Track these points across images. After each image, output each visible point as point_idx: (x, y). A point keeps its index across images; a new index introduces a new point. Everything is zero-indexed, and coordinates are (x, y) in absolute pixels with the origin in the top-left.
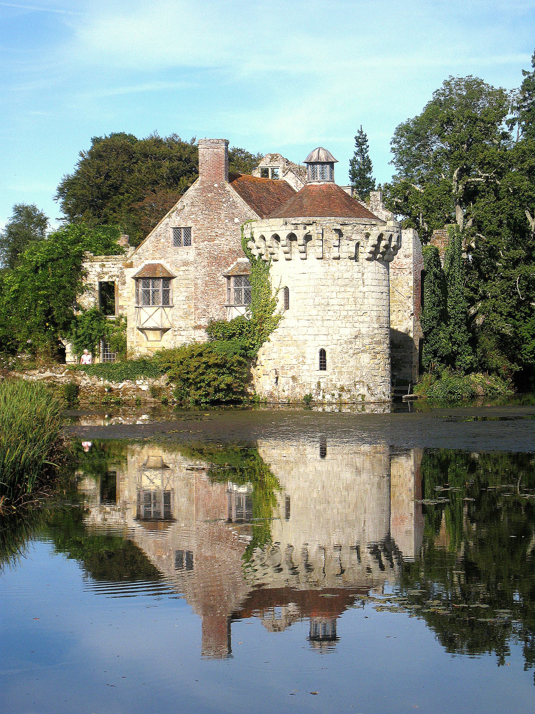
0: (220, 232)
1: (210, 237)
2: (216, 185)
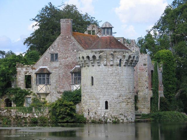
2: (67, 37)
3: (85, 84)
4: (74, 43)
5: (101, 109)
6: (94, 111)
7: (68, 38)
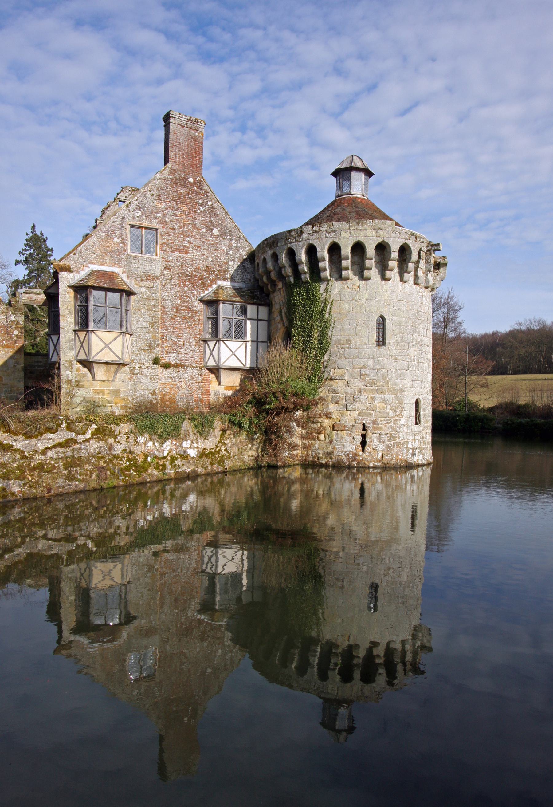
0: (195, 244)
1: (182, 248)
2: (191, 180)
3: (349, 342)
4: (212, 207)
5: (406, 426)
6: (385, 430)
7: (195, 182)
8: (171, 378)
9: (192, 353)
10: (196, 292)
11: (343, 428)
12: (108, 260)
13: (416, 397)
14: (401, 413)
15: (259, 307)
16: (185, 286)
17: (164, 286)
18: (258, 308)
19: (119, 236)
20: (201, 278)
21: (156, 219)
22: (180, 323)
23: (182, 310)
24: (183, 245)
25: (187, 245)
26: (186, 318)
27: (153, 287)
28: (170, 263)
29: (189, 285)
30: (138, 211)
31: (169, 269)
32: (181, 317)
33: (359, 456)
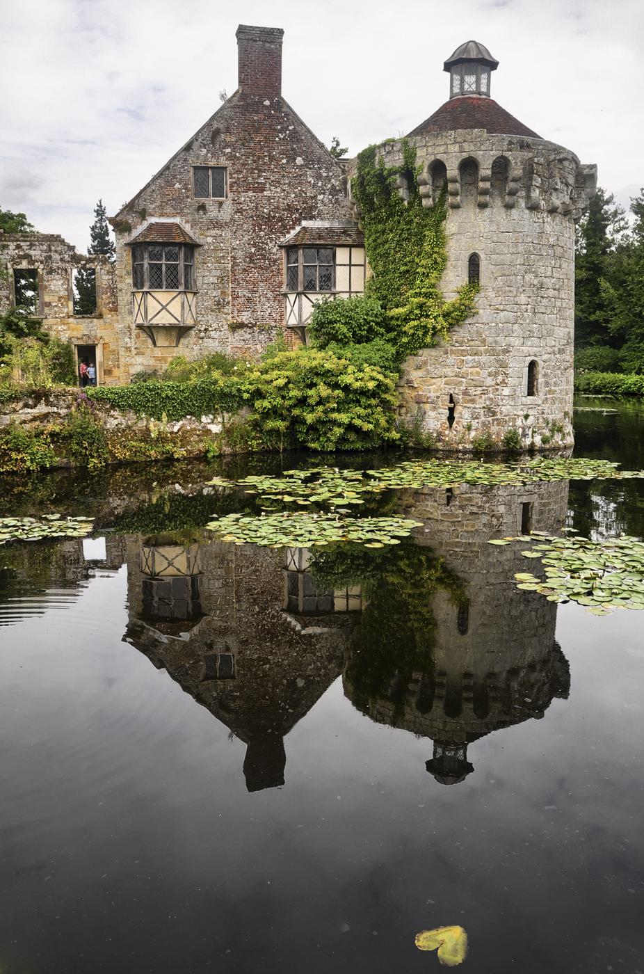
0: (272, 179)
1: (256, 185)
2: (267, 103)
6: (481, 402)
8: (244, 340)
9: (269, 310)
10: (274, 236)
11: (425, 400)
12: (169, 210)
13: (529, 359)
14: (504, 380)
15: (353, 249)
16: (261, 230)
17: (235, 233)
18: (350, 250)
19: (180, 181)
20: (281, 219)
21: (224, 155)
22: (255, 275)
23: (258, 259)
24: (257, 183)
25: (263, 181)
26: (262, 269)
27: (221, 235)
28: (241, 206)
29: (265, 229)
30: (202, 150)
31: (239, 212)
32: (255, 268)
33: (445, 435)
